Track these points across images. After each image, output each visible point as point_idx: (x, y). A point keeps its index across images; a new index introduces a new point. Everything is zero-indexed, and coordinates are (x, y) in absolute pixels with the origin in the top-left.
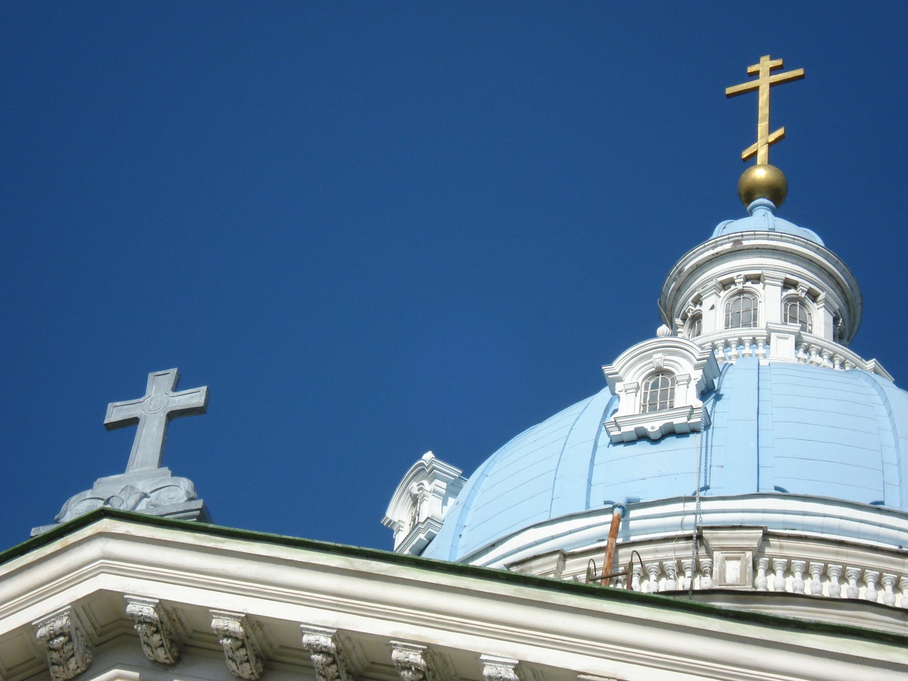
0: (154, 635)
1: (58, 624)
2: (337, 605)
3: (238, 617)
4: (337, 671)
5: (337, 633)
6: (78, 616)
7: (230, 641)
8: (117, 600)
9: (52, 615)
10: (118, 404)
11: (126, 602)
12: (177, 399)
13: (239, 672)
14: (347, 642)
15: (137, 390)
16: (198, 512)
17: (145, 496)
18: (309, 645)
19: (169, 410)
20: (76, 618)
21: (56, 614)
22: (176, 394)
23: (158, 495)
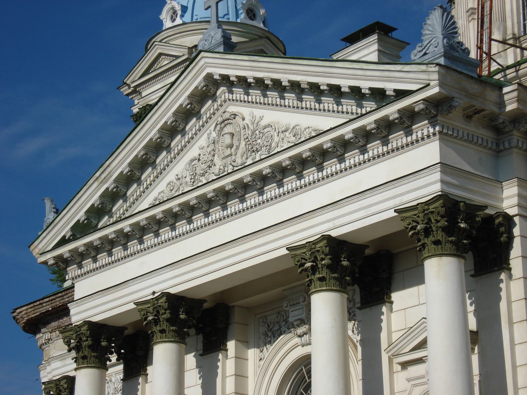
6: (207, 80)
20: (206, 81)
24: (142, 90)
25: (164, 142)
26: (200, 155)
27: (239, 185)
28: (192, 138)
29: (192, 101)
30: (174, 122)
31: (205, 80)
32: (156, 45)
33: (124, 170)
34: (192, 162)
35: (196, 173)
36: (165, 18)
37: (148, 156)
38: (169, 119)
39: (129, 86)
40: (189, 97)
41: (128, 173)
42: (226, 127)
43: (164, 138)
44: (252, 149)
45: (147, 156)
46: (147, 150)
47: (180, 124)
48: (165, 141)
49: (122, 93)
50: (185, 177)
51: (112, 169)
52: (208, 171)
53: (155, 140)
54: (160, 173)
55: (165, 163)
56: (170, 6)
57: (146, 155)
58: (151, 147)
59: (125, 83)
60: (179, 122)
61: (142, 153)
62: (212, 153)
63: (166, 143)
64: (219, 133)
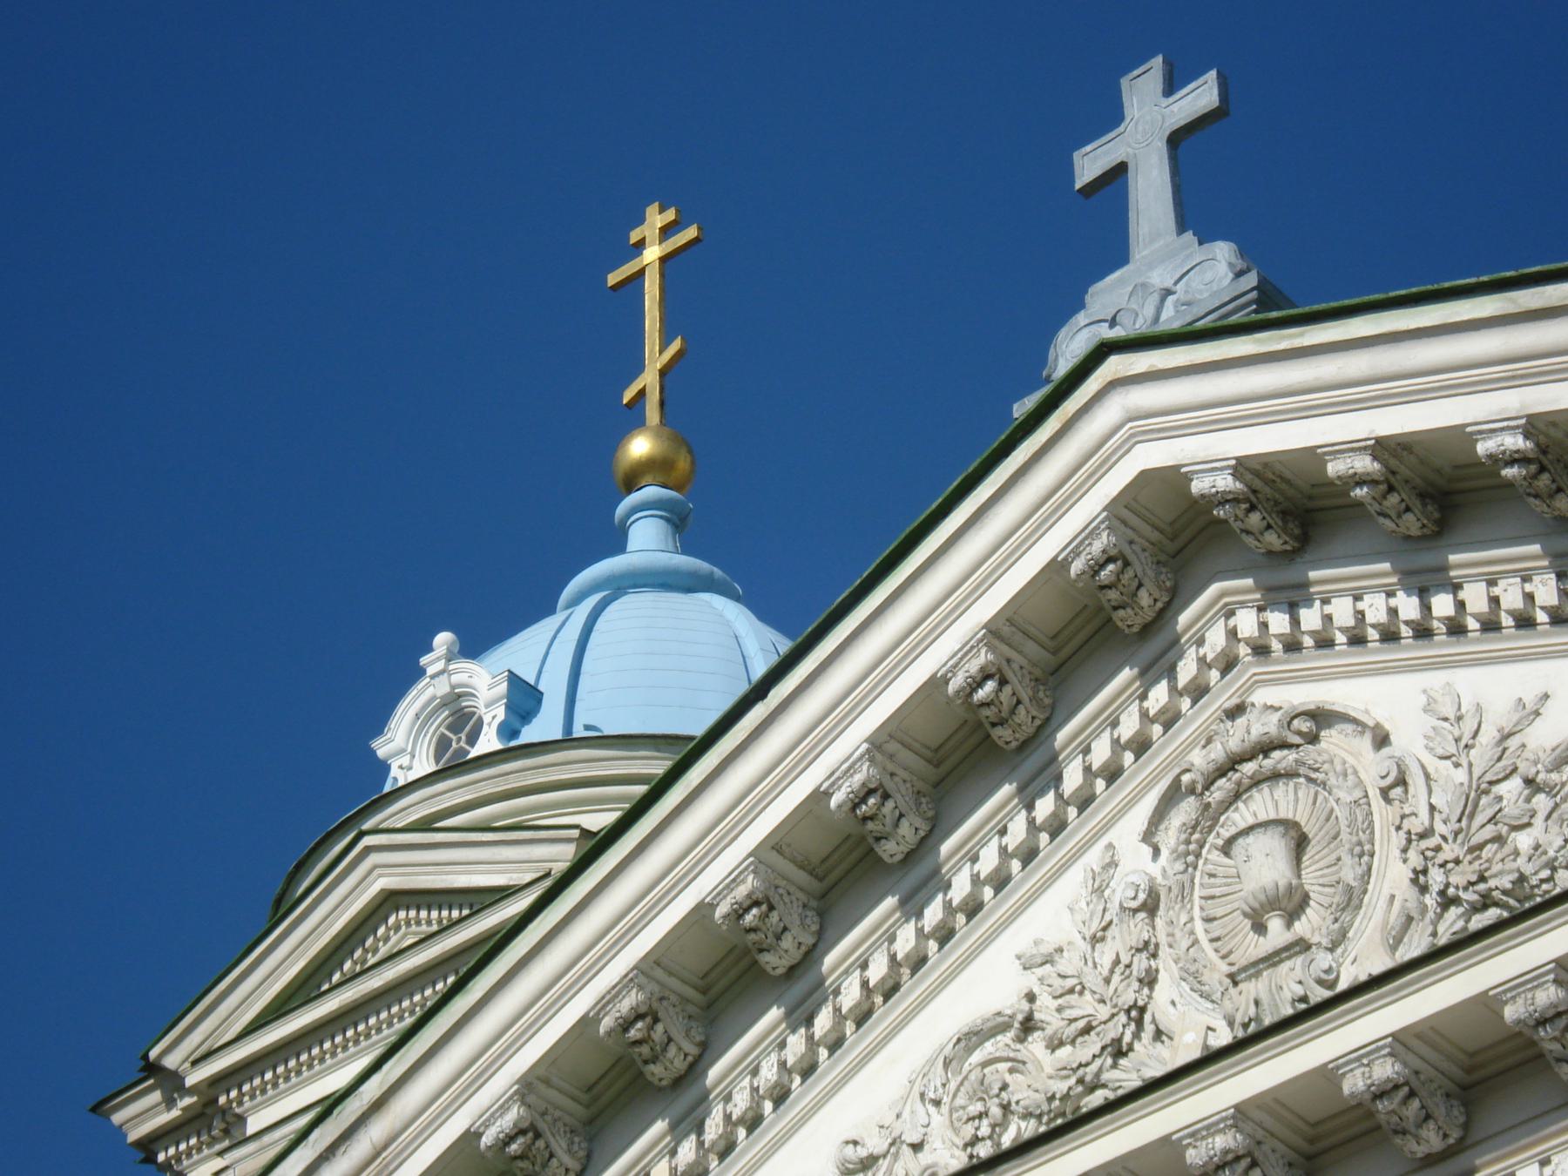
0: (1250, 515)
1: (1097, 546)
2: (1513, 378)
3: (1365, 448)
4: (1554, 481)
5: (1528, 422)
6: (1124, 522)
7: (1365, 489)
8: (1171, 479)
9: (1083, 535)
10: (1088, 148)
11: (1188, 478)
12: (1175, 108)
13: (1402, 530)
14: (1552, 432)
15: (1110, 116)
16: (1254, 294)
17: (1168, 292)
18: (1490, 456)
19: (1167, 133)
20: (1122, 528)
21: (1088, 533)
22: (1171, 99)
23: (1187, 284)
24: (247, 1105)
25: (778, 938)
26: (1031, 997)
27: (1433, 1072)
28: (973, 908)
29: (1008, 661)
30: (870, 792)
31: (1116, 523)
32: (369, 850)
33: (487, 1125)
34: (970, 1051)
35: (1006, 1108)
36: (402, 751)
37: (660, 1028)
38: (836, 778)
39: (172, 1083)
40: (994, 632)
41: (510, 1139)
42: (1240, 804)
43: (780, 906)
44: (1482, 887)
45: (651, 1028)
46: (656, 988)
47: (901, 815)
48: (785, 929)
49: (119, 1132)
50: (917, 1147)
51: (398, 1125)
52: (1105, 1076)
53: (726, 916)
54: (721, 1145)
55: (769, 1073)
56: (441, 688)
57: (649, 1020)
58: (684, 981)
59: (152, 1069)
60: (901, 802)
61: (626, 1004)
62: (1141, 963)
63: (787, 942)
64: (1188, 842)
